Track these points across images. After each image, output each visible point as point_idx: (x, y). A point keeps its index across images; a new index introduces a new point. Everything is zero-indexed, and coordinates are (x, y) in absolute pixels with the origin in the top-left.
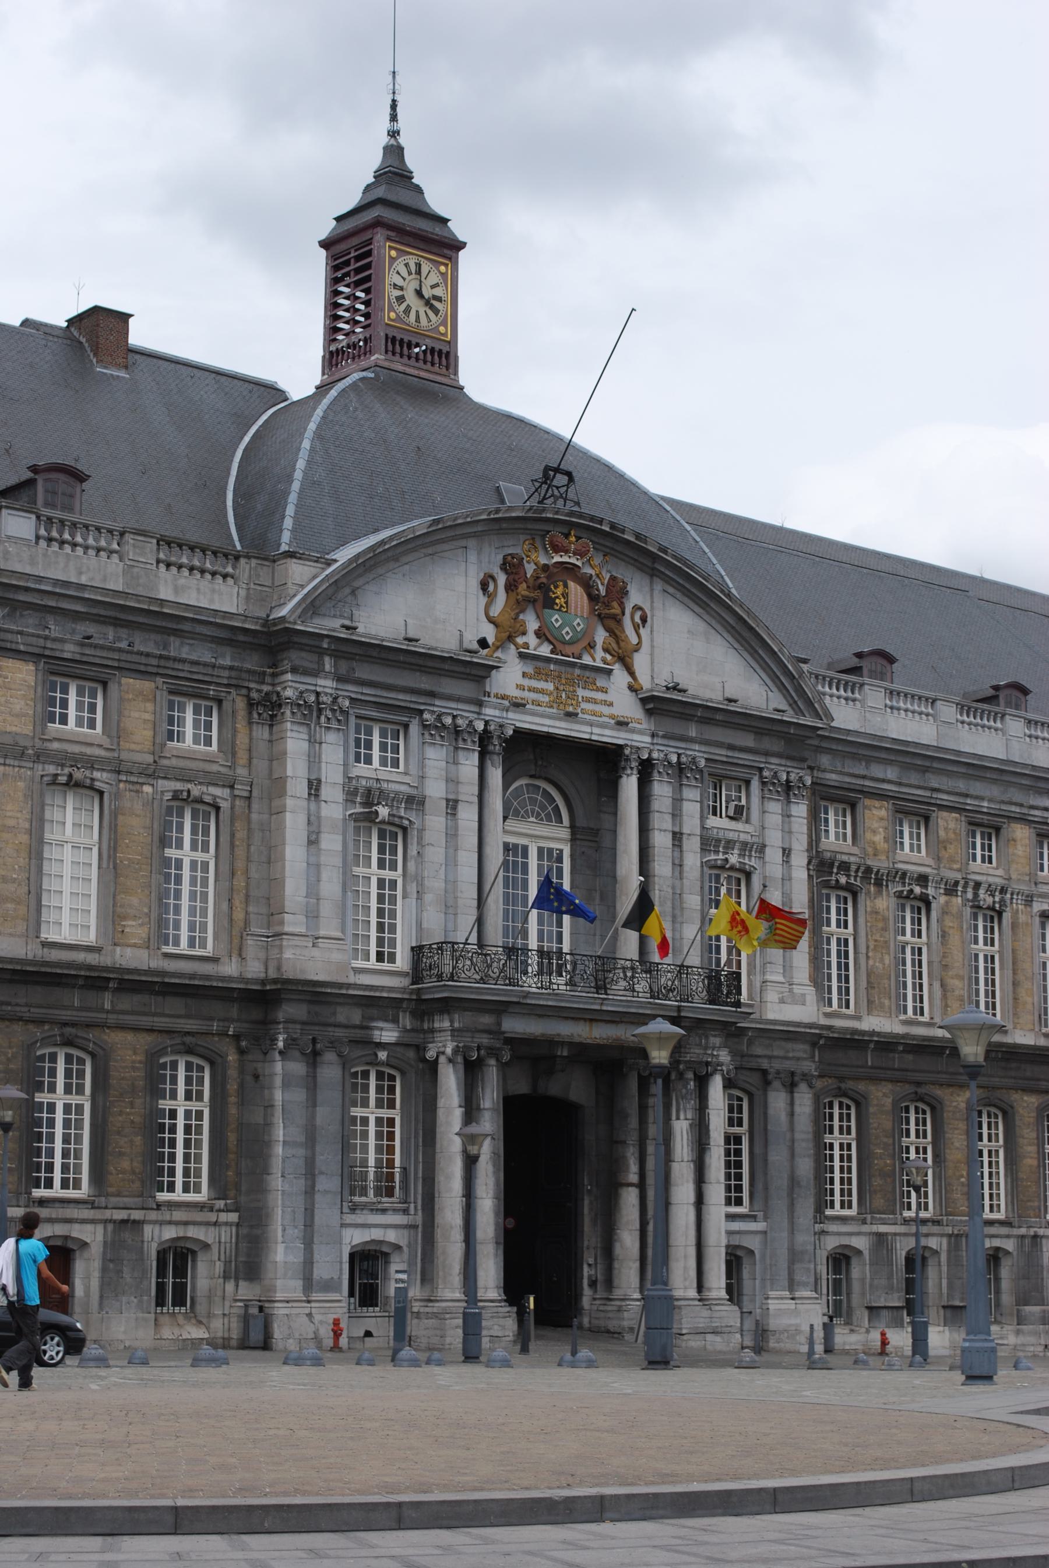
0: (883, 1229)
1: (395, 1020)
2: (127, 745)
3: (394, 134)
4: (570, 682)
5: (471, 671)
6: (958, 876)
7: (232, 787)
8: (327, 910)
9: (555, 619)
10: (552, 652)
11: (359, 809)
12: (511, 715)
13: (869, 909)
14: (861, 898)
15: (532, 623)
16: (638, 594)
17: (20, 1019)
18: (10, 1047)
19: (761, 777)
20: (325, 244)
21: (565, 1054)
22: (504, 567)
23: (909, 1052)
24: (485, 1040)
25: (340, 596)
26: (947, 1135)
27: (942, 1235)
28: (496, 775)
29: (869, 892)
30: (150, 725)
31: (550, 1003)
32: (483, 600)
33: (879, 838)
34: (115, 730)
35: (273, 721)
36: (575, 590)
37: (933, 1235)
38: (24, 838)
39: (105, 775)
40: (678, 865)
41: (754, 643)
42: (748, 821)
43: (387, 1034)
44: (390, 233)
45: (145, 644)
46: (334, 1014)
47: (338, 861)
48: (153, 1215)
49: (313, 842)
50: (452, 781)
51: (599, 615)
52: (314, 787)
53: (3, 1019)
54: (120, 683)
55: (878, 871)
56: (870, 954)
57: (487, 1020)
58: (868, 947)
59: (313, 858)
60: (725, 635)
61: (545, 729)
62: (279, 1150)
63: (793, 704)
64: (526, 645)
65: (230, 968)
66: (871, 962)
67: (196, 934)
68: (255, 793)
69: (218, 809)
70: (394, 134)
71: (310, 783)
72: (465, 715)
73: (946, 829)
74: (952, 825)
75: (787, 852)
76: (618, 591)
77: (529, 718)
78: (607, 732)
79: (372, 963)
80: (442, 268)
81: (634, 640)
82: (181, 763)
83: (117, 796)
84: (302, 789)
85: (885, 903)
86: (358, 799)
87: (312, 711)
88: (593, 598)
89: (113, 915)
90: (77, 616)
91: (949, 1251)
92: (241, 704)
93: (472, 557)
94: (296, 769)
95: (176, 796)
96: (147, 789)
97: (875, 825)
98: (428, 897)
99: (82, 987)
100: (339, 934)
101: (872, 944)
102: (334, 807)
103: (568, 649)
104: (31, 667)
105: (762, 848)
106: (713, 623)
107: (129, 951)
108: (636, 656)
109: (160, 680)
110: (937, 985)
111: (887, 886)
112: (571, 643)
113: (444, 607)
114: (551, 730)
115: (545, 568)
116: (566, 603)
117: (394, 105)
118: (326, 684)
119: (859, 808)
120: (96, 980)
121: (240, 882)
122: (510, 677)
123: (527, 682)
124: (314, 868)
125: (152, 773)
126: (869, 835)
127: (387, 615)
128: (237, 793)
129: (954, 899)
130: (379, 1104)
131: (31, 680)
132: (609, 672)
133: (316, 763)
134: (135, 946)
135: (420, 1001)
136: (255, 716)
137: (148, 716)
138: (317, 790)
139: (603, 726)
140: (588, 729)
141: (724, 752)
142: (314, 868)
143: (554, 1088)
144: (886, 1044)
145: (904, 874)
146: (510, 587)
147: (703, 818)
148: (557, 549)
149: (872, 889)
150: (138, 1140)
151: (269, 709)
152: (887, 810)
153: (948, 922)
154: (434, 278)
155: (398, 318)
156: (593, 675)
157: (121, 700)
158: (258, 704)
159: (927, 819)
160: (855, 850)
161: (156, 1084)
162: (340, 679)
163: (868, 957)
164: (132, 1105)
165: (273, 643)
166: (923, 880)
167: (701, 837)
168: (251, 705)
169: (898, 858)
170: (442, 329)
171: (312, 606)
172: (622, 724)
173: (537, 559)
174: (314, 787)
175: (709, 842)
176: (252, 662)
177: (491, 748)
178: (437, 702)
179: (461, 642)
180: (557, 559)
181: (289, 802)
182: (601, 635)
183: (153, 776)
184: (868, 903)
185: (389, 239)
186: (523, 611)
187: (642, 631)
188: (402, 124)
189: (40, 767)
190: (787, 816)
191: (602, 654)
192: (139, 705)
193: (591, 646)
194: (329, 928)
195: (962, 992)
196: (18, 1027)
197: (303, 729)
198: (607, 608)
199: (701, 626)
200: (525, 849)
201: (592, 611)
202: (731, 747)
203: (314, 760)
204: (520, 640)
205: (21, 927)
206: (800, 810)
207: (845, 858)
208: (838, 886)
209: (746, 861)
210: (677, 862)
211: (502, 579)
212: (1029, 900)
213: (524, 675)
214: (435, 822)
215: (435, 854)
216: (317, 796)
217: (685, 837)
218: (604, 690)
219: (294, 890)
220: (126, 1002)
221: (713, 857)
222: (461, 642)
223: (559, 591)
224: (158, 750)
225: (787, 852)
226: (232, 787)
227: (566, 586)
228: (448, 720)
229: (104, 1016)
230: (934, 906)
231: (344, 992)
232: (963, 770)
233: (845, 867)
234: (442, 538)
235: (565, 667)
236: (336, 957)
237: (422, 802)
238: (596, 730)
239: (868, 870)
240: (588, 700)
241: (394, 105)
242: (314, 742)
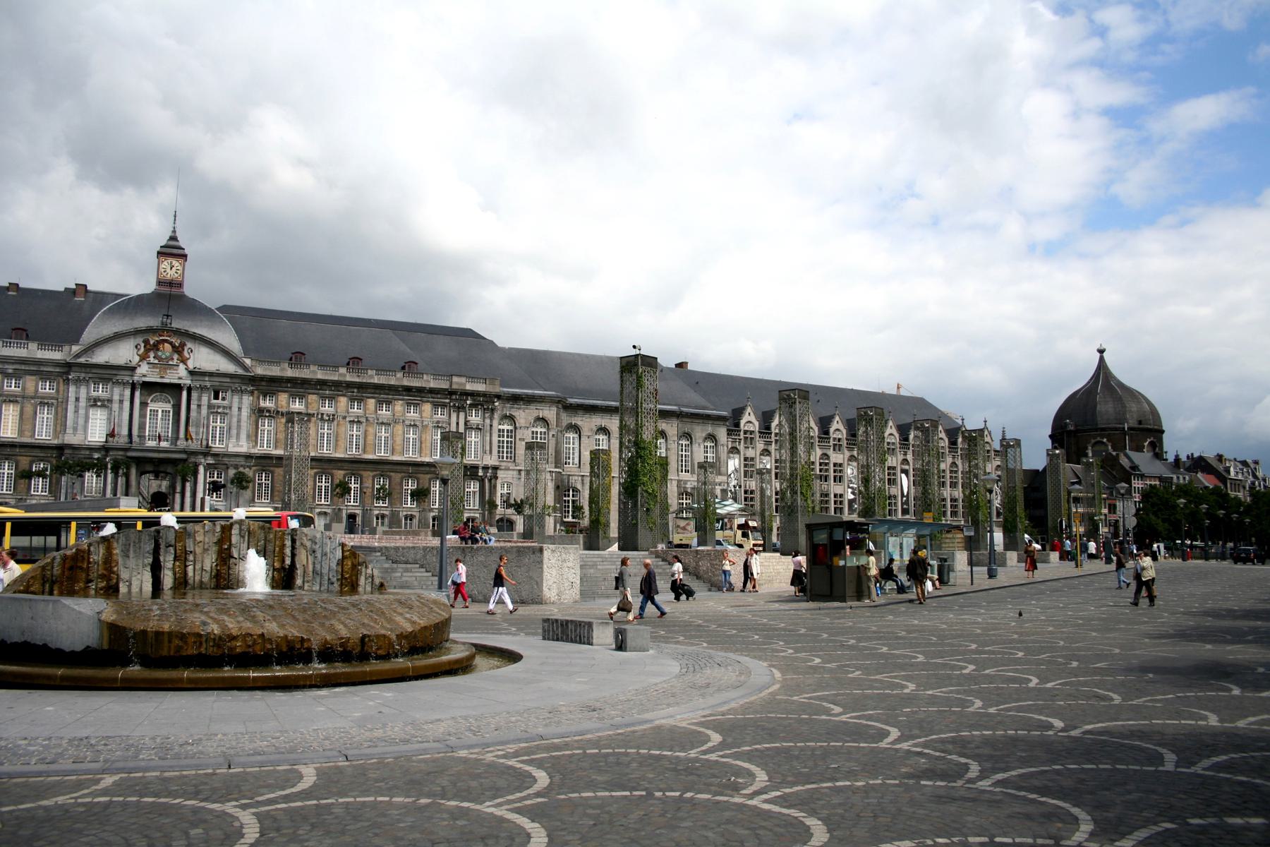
15: (152, 354)
16: (189, 345)
34: (24, 389)
49: (76, 411)
50: (122, 395)
52: (77, 399)
67: (44, 432)
72: (127, 378)
75: (240, 409)
76: (183, 345)
87: (78, 382)
88: (173, 346)
102: (83, 403)
120: (12, 445)
122: (144, 369)
125: (32, 398)
127: (103, 356)
133: (78, 394)
151: (67, 381)
165: (68, 366)
171: (78, 356)
174: (77, 399)
175: (210, 406)
182: (176, 356)
198: (178, 350)
212: (344, 418)
219: (70, 422)
225: (240, 409)
233: (269, 411)
234: (118, 337)
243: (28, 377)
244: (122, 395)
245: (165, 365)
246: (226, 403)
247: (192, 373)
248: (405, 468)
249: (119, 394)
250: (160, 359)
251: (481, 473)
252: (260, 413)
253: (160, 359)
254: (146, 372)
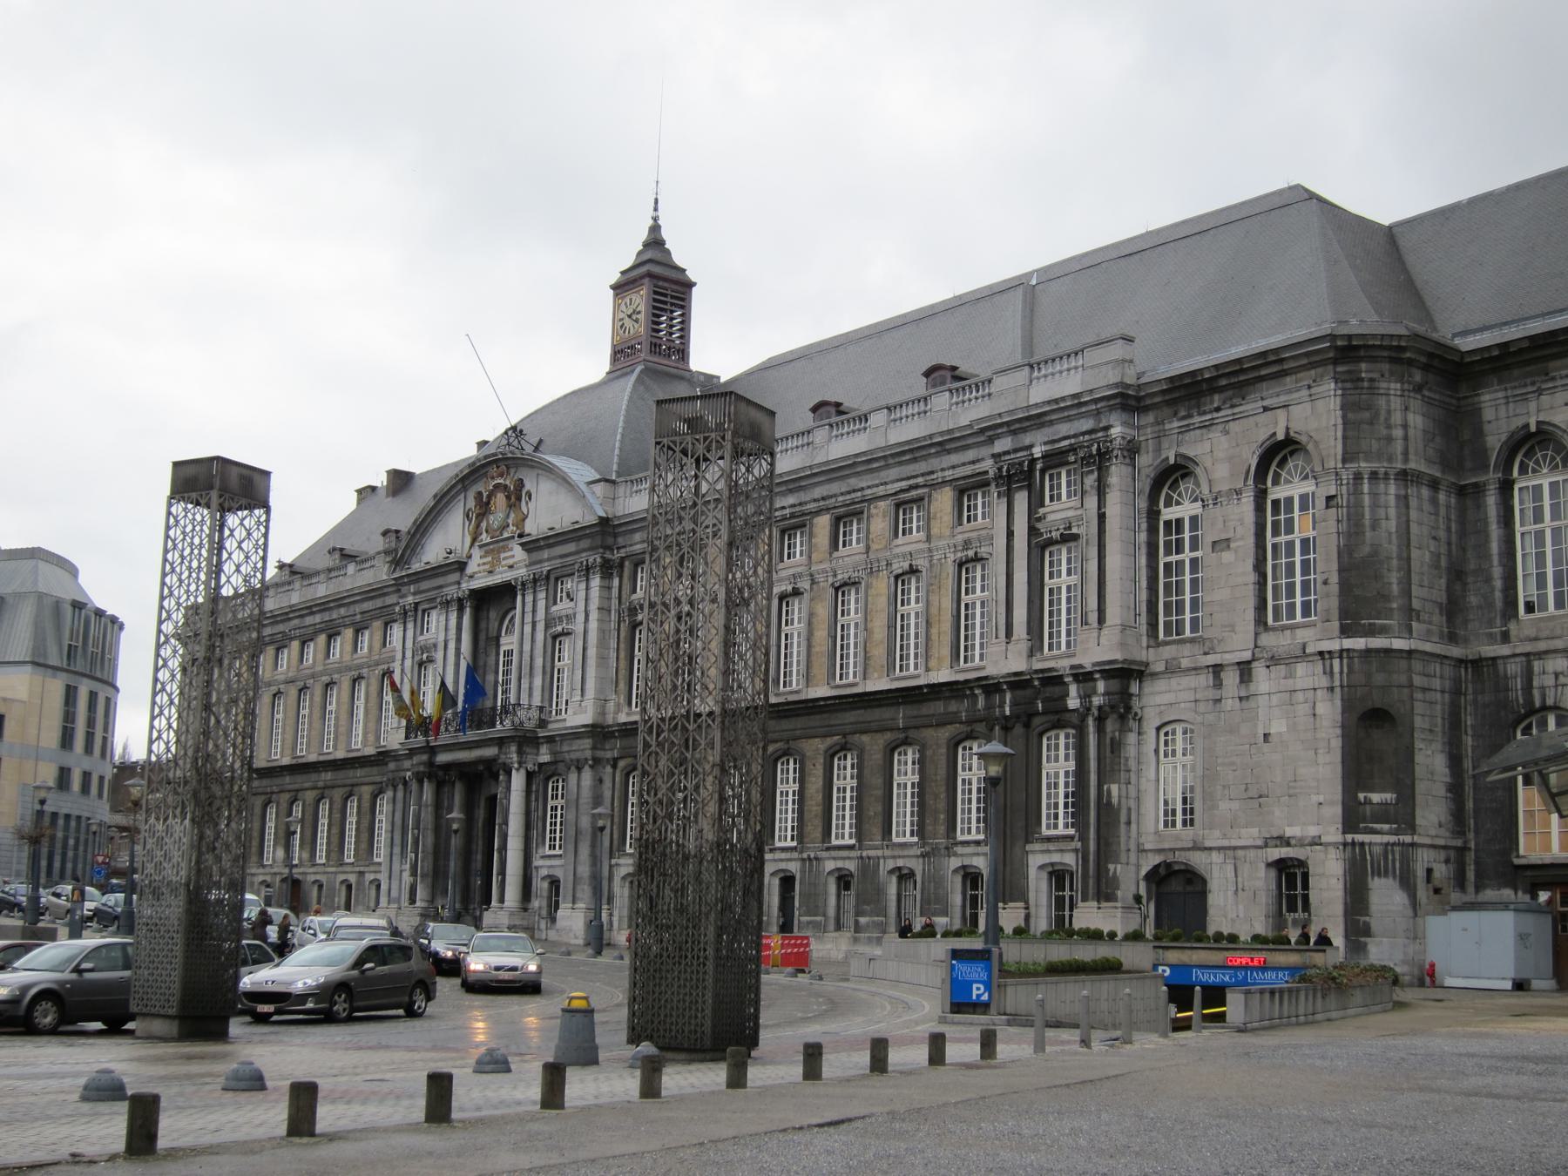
70: (655, 219)
117: (656, 201)
162: (414, 594)
188: (660, 213)
241: (656, 201)
248: (884, 714)
251: (1073, 703)
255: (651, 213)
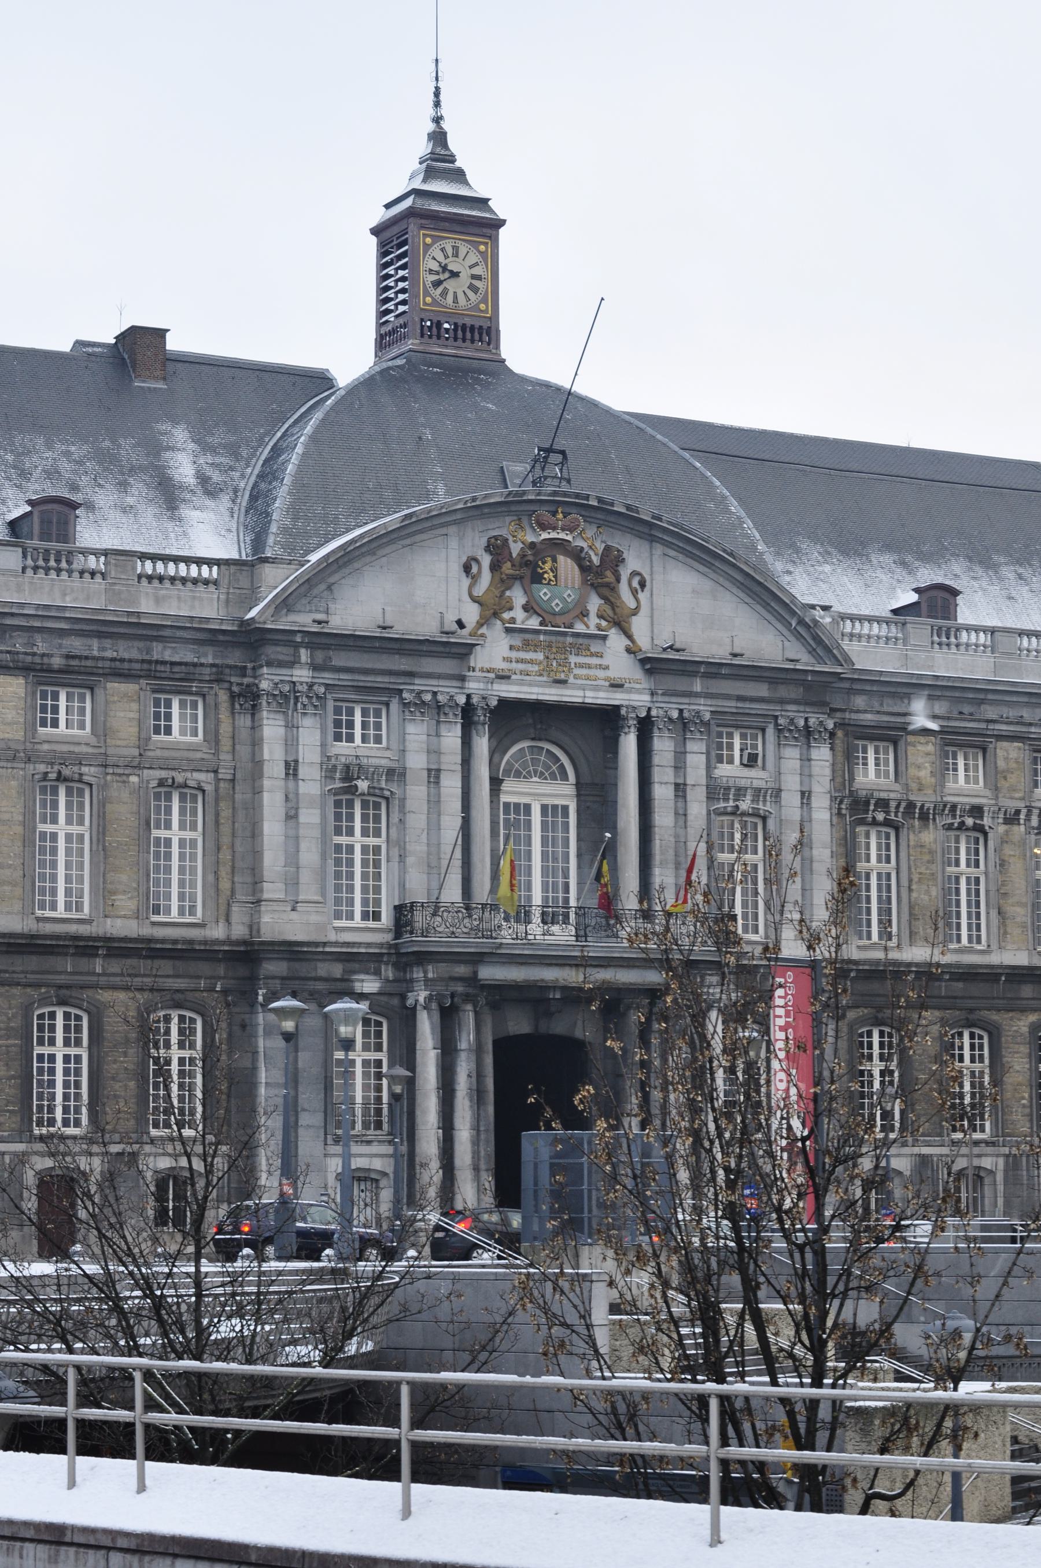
0: (926, 1150)
1: (377, 973)
2: (113, 742)
3: (437, 120)
4: (563, 650)
5: (454, 650)
6: (1021, 805)
7: (216, 772)
8: (306, 877)
9: (543, 593)
10: (541, 624)
11: (338, 785)
12: (496, 686)
13: (912, 843)
14: (903, 833)
16: (636, 558)
17: (18, 984)
18: (10, 1008)
19: (777, 724)
20: (376, 231)
21: (558, 996)
22: (487, 549)
23: (958, 980)
24: (460, 988)
25: (315, 591)
26: (1005, 1060)
27: (998, 1156)
28: (482, 744)
29: (913, 826)
30: (135, 723)
31: (526, 952)
32: (466, 582)
33: (925, 774)
34: (102, 730)
35: (254, 710)
36: (566, 564)
37: (986, 1155)
38: (19, 829)
39: (92, 769)
40: (681, 815)
41: (766, 596)
42: (764, 768)
43: (370, 985)
44: (423, 221)
45: (128, 651)
46: (316, 969)
47: (316, 833)
48: (148, 1148)
49: (291, 816)
50: (435, 752)
51: (592, 585)
52: (292, 769)
53: (3, 985)
54: (105, 688)
55: (923, 806)
56: (914, 887)
57: (462, 970)
58: (910, 881)
59: (290, 830)
60: (735, 590)
61: (534, 697)
62: (262, 1091)
63: (812, 652)
64: (513, 620)
65: (217, 932)
66: (914, 895)
67: (183, 904)
68: (238, 776)
69: (204, 791)
70: (437, 120)
71: (287, 764)
72: (446, 690)
73: (1006, 759)
74: (1013, 754)
75: (806, 796)
76: (613, 560)
77: (515, 688)
78: (602, 694)
79: (358, 921)
80: (482, 248)
81: (632, 604)
82: (166, 754)
83: (105, 786)
84: (280, 770)
85: (930, 836)
86: (338, 775)
87: (288, 700)
89: (104, 892)
90: (62, 633)
91: (1006, 1171)
92: (223, 697)
93: (454, 543)
94: (273, 753)
95: (161, 783)
96: (134, 779)
97: (920, 760)
98: (410, 860)
99: (73, 955)
100: (319, 898)
101: (915, 877)
102: (311, 784)
103: (559, 620)
104: (21, 681)
105: (777, 793)
106: (721, 580)
107: (119, 922)
108: (634, 620)
109: (143, 682)
110: (994, 913)
111: (934, 819)
112: (562, 613)
113: (427, 591)
114: (541, 697)
115: (532, 545)
116: (555, 577)
117: (437, 93)
118: (302, 675)
119: (901, 744)
120: (84, 947)
121: (226, 855)
122: (495, 650)
123: (514, 655)
124: (293, 841)
126: (912, 771)
128: (220, 776)
129: (1015, 828)
130: (366, 1048)
131: (22, 692)
132: (604, 638)
133: (293, 745)
134: (125, 917)
135: (399, 954)
136: (237, 706)
137: (132, 715)
138: (296, 770)
139: (596, 688)
140: (580, 693)
141: (733, 704)
142: (293, 841)
143: (559, 1027)
144: (927, 973)
145: (954, 807)
146: (494, 567)
147: (709, 768)
148: (544, 527)
149: (917, 823)
150: (132, 1084)
151: (248, 699)
152: (934, 744)
153: (1008, 850)
154: (473, 258)
155: (435, 302)
156: (585, 641)
157: (107, 702)
158: (240, 695)
159: (984, 750)
160: (897, 787)
161: (148, 1036)
162: (315, 667)
163: (910, 890)
164: (125, 1054)
166: (977, 811)
167: (707, 786)
168: (233, 697)
169: (946, 791)
170: (482, 306)
171: (285, 604)
172: (616, 686)
173: (521, 538)
174: (292, 769)
175: (715, 791)
176: (235, 658)
177: (476, 718)
178: (417, 681)
179: (442, 623)
180: (545, 535)
181: (267, 783)
182: (594, 603)
183: (138, 767)
184: (912, 837)
185: (423, 227)
186: (509, 588)
187: (641, 596)
188: (444, 111)
189: (32, 766)
190: (806, 760)
191: (597, 621)
192: (125, 705)
193: (584, 614)
194: (308, 891)
195: (1024, 919)
196: (16, 991)
197: (280, 716)
199: (707, 584)
200: (528, 808)
201: (584, 582)
202: (740, 698)
203: (291, 743)
204: (506, 616)
205: (17, 906)
206: (822, 754)
207: (883, 795)
208: (875, 823)
209: (761, 806)
210: (681, 812)
211: (486, 560)
213: (511, 648)
214: (417, 792)
215: (417, 821)
216: (295, 775)
217: (688, 788)
218: (600, 655)
219: (272, 860)
220: (115, 966)
221: (722, 805)
222: (442, 623)
223: (547, 567)
224: (143, 743)
225: (806, 796)
226: (216, 772)
227: (554, 560)
228: (428, 697)
229: (95, 978)
230: (990, 835)
231: (320, 949)
232: (1025, 699)
235: (557, 638)
236: (314, 918)
237: (403, 774)
238: (589, 694)
239: (911, 805)
240: (581, 666)
241: (437, 93)
242: (291, 727)
243: (116, 687)
244: (435, 752)
245: (557, 638)
246: (757, 777)
247: (652, 666)
249: (420, 743)
250: (546, 616)
252: (856, 809)
253: (546, 616)
254: (503, 666)
255: (431, 112)
